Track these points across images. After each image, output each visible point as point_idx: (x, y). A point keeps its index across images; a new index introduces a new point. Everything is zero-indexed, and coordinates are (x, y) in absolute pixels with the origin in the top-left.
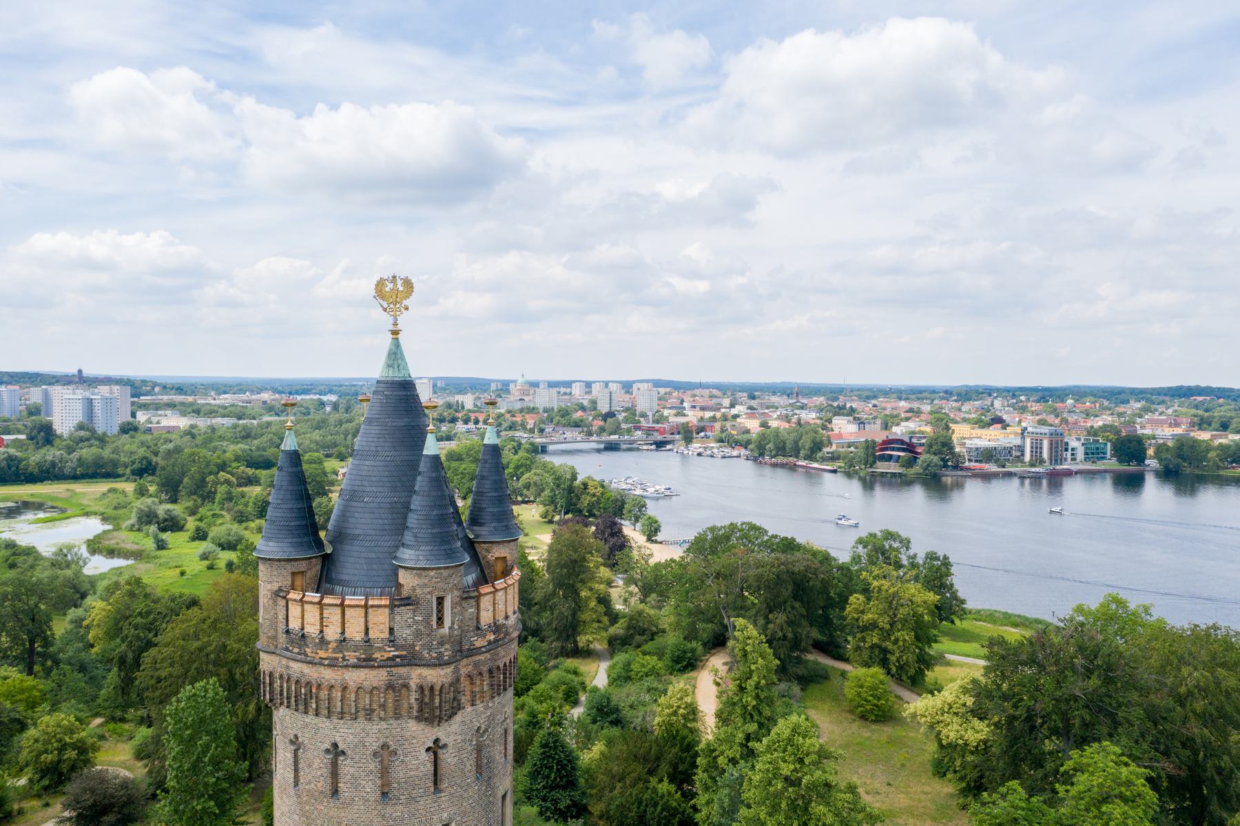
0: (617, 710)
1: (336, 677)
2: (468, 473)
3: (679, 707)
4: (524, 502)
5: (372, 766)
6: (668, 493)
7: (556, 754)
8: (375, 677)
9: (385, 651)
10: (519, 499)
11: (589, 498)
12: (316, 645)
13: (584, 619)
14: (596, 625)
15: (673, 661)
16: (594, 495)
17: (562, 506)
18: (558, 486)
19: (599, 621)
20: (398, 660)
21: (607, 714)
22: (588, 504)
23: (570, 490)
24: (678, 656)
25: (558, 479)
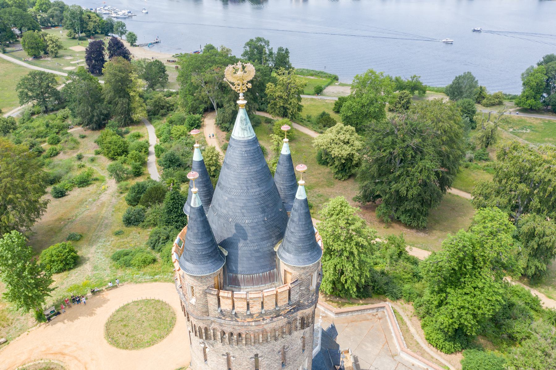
0: (178, 160)
1: (259, 329)
2: (18, 14)
3: (212, 156)
4: (52, 26)
5: (278, 357)
6: (130, 15)
7: (179, 201)
8: (281, 321)
9: (286, 309)
10: (49, 25)
11: (93, 24)
12: (244, 316)
13: (134, 106)
14: (140, 109)
15: (190, 125)
16: (95, 22)
17: (79, 29)
18: (74, 18)
19: (142, 106)
20: (292, 310)
21: (175, 163)
22: (93, 27)
23: (82, 21)
24: (192, 123)
25: (73, 14)
